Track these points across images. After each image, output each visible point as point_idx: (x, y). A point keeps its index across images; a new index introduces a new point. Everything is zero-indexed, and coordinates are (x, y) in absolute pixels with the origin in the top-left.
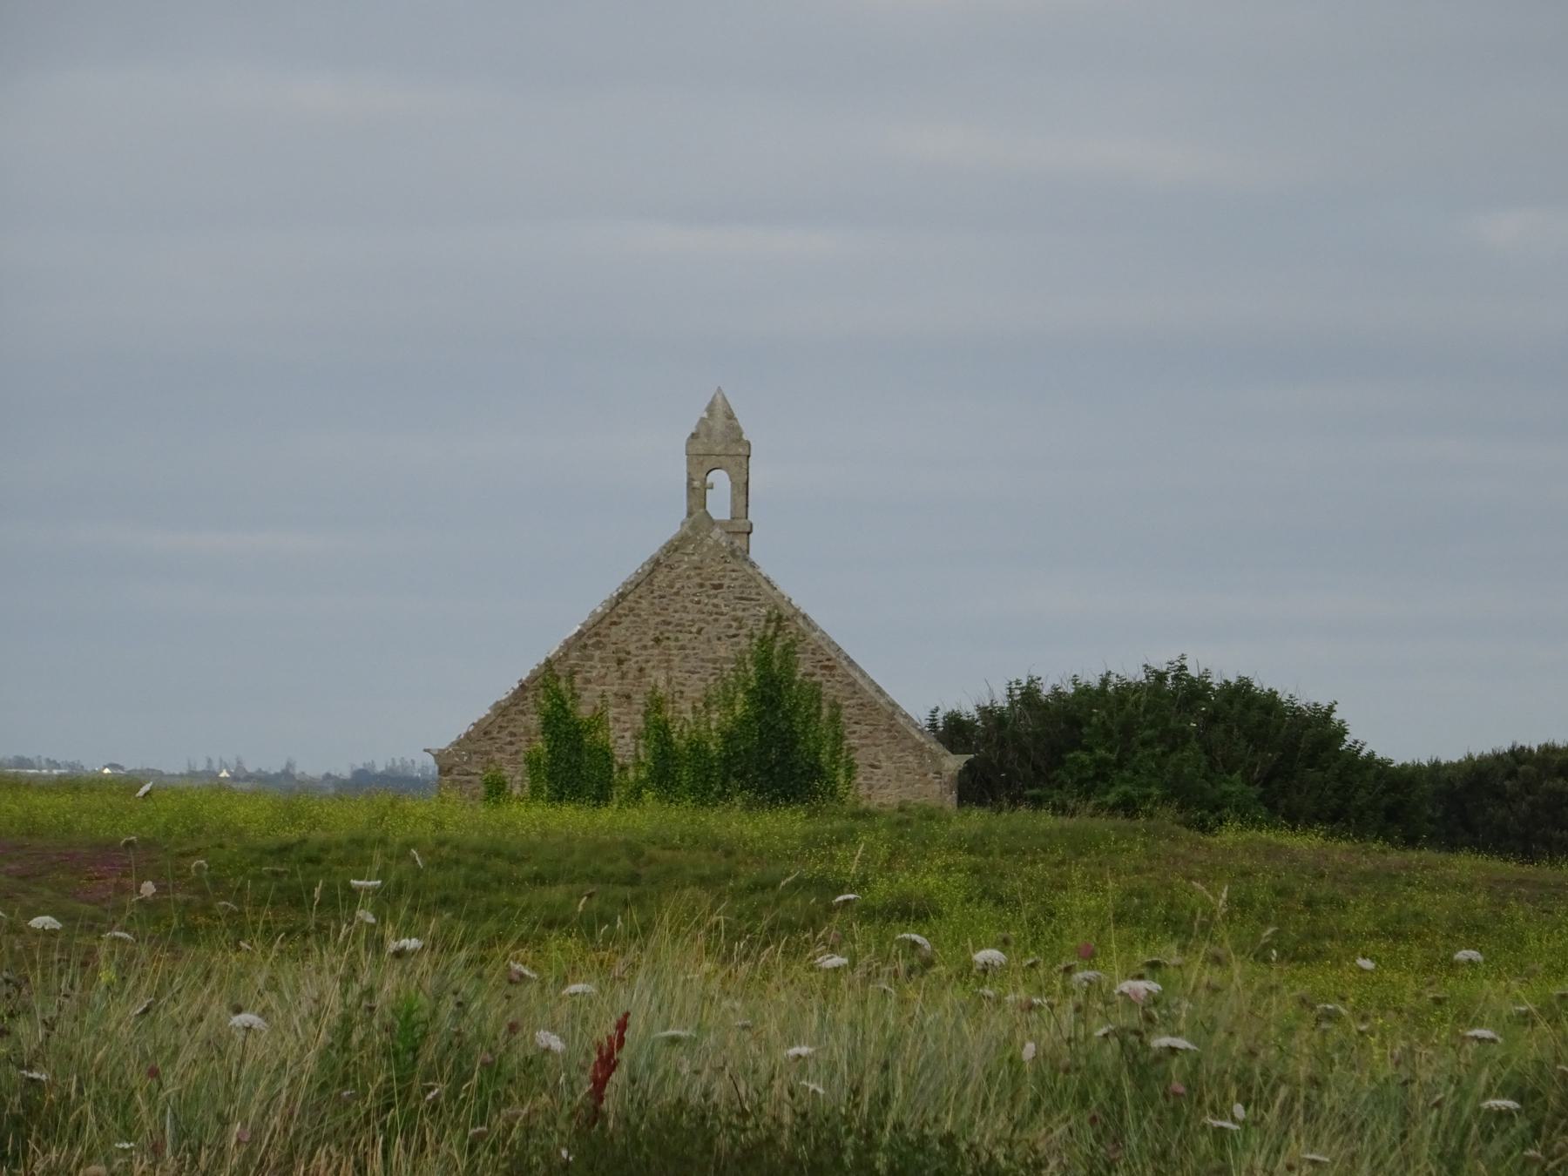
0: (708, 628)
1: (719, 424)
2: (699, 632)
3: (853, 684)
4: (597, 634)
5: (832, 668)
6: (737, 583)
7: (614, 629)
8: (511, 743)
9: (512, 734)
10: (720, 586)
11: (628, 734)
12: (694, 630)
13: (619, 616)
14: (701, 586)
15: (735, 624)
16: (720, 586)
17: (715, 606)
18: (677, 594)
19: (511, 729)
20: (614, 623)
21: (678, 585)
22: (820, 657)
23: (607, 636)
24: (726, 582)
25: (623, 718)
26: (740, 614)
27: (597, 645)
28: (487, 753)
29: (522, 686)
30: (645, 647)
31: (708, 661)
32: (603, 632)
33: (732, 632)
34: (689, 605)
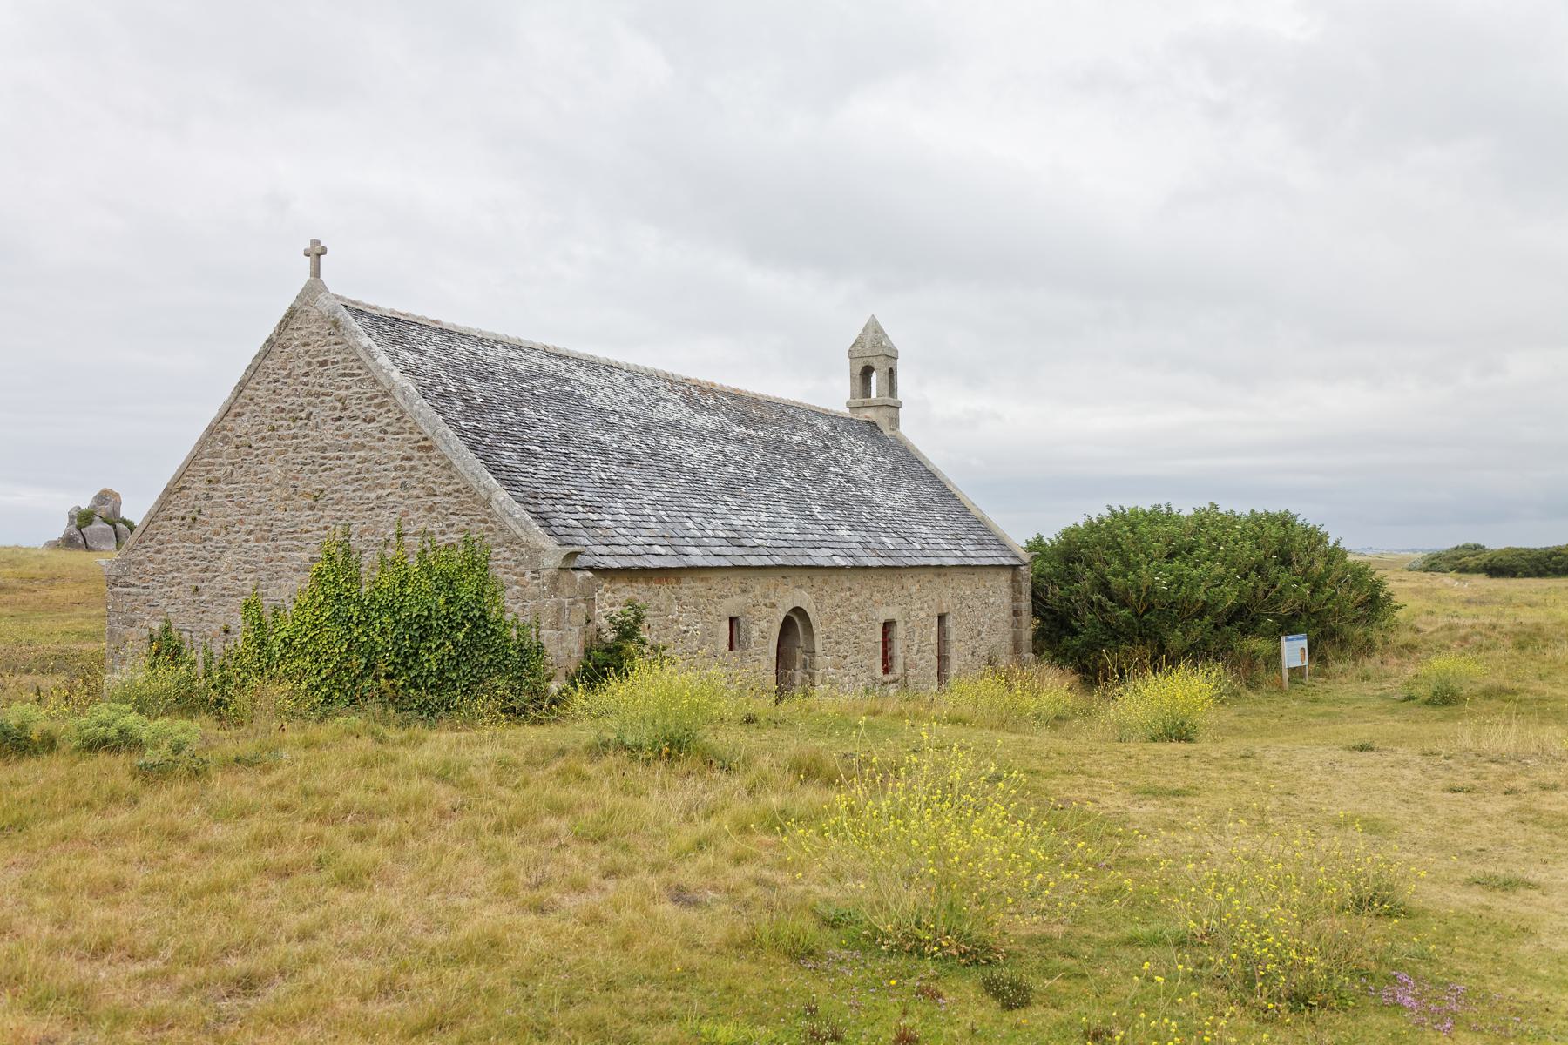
1: (871, 335)
2: (308, 418)
3: (449, 466)
4: (224, 428)
5: (429, 448)
6: (339, 358)
7: (239, 420)
8: (159, 552)
9: (161, 543)
10: (323, 364)
11: (251, 537)
12: (303, 415)
14: (309, 364)
15: (339, 405)
16: (323, 364)
17: (321, 386)
18: (288, 376)
19: (159, 537)
20: (238, 415)
22: (416, 437)
23: (231, 430)
24: (331, 357)
25: (247, 520)
26: (343, 393)
27: (225, 440)
28: (141, 563)
29: (168, 491)
31: (317, 449)
33: (338, 414)
34: (300, 387)
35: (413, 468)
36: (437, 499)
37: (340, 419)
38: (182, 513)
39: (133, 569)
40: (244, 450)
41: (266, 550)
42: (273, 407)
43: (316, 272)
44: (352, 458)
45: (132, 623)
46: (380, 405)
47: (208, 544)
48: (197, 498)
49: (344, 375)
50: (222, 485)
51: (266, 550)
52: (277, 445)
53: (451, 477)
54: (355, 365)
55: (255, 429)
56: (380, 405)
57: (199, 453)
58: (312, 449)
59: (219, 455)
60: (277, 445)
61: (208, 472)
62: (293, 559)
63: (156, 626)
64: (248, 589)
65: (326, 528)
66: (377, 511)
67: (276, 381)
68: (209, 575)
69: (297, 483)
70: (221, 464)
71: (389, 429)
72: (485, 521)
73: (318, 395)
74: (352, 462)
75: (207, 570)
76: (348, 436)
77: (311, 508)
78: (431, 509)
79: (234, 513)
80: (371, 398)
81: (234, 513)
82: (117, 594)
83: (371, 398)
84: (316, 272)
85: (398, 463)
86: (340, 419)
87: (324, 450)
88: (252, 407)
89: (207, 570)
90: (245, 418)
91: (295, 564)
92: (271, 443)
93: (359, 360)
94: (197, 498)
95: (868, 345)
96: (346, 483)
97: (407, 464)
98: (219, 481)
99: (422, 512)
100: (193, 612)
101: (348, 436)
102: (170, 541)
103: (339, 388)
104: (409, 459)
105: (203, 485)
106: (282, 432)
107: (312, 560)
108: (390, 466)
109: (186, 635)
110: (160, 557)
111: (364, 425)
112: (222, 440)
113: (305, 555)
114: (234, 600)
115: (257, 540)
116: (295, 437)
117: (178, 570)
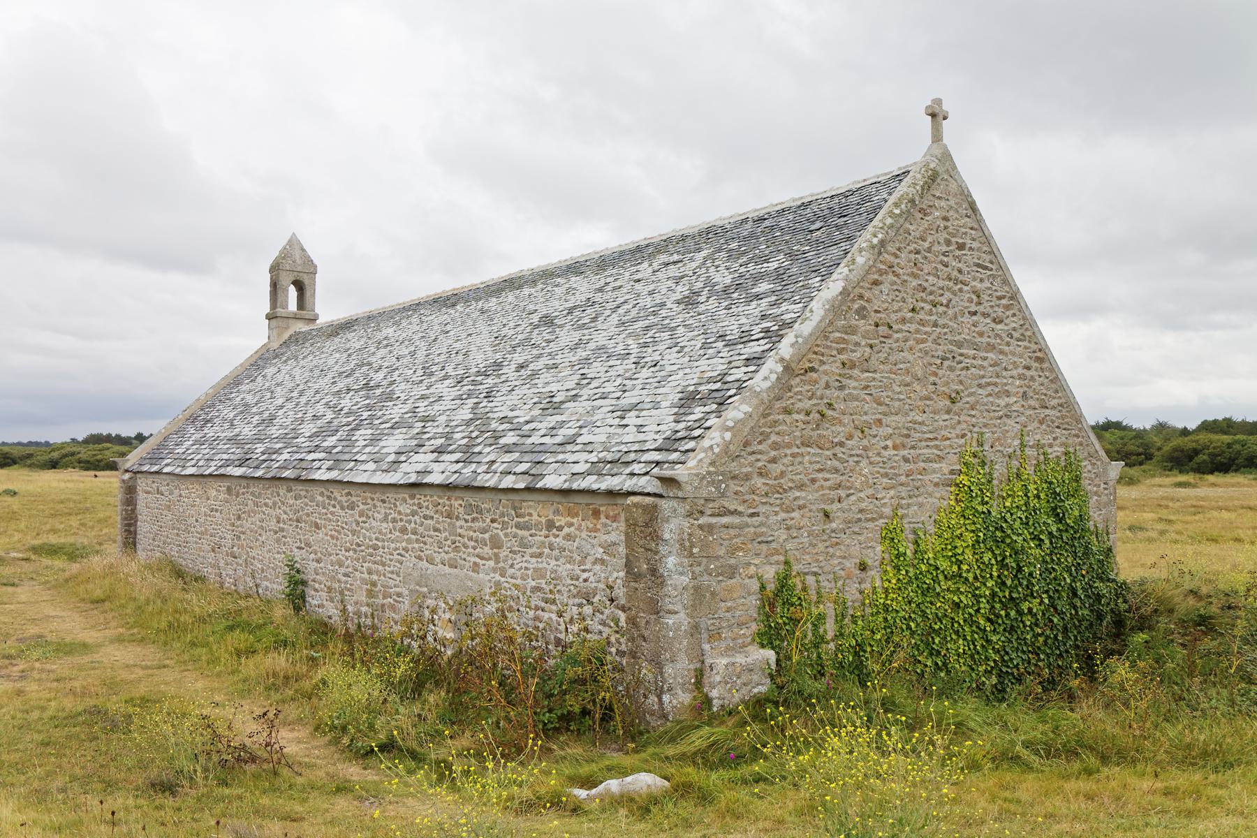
0: (955, 299)
4: (861, 297)
8: (774, 461)
9: (775, 446)
10: (961, 247)
11: (889, 443)
13: (881, 272)
16: (961, 247)
18: (929, 250)
19: (774, 438)
20: (876, 283)
21: (930, 239)
27: (862, 313)
28: (747, 477)
30: (903, 321)
32: (867, 294)
33: (973, 309)
35: (1032, 378)
36: (1047, 412)
37: (975, 313)
38: (807, 404)
39: (734, 486)
40: (883, 330)
41: (906, 460)
42: (915, 283)
43: (937, 136)
44: (985, 359)
45: (732, 572)
46: (1007, 307)
47: (838, 450)
48: (827, 386)
49: (978, 265)
50: (856, 372)
51: (906, 460)
52: (917, 331)
53: (1057, 392)
54: (988, 257)
55: (896, 306)
56: (1007, 307)
57: (831, 323)
58: (951, 342)
59: (852, 330)
60: (917, 331)
61: (840, 351)
62: (934, 471)
63: (770, 573)
64: (887, 511)
65: (963, 436)
66: (1005, 419)
67: (918, 252)
68: (843, 493)
69: (937, 380)
70: (857, 344)
71: (1016, 335)
72: (1078, 436)
73: (956, 282)
74: (985, 363)
75: (839, 486)
76: (981, 334)
77: (948, 412)
78: (1041, 422)
79: (871, 411)
80: (999, 298)
81: (871, 411)
82: (710, 528)
83: (999, 298)
84: (937, 136)
85: (1020, 371)
86: (975, 313)
87: (959, 345)
88: (891, 277)
89: (839, 486)
90: (885, 288)
91: (935, 477)
92: (913, 327)
93: (992, 252)
94: (827, 386)
95: (299, 262)
96: (980, 386)
97: (1028, 373)
98: (853, 366)
99: (1036, 424)
100: (821, 546)
101: (981, 334)
102: (789, 446)
103: (974, 279)
104: (1028, 368)
105: (835, 368)
106: (922, 316)
107: (952, 472)
108: (1014, 373)
109: (810, 580)
110: (776, 469)
111: (993, 325)
112: (858, 312)
113: (945, 467)
114: (870, 525)
115: (895, 447)
116: (935, 325)
117: (801, 487)
